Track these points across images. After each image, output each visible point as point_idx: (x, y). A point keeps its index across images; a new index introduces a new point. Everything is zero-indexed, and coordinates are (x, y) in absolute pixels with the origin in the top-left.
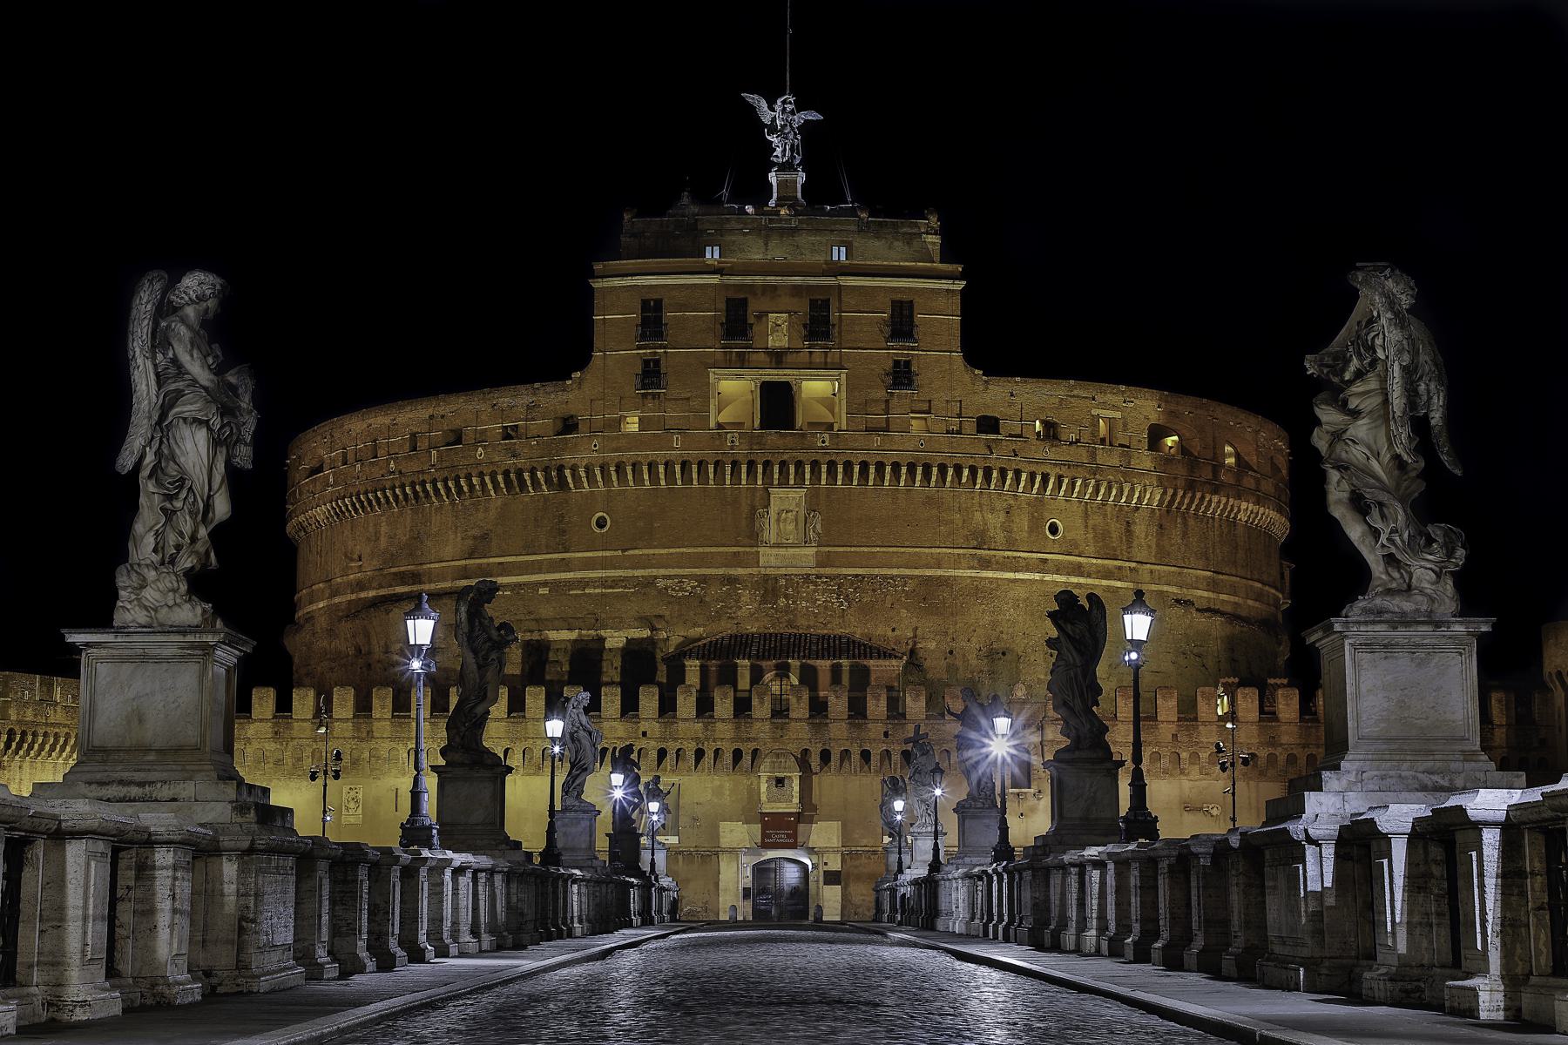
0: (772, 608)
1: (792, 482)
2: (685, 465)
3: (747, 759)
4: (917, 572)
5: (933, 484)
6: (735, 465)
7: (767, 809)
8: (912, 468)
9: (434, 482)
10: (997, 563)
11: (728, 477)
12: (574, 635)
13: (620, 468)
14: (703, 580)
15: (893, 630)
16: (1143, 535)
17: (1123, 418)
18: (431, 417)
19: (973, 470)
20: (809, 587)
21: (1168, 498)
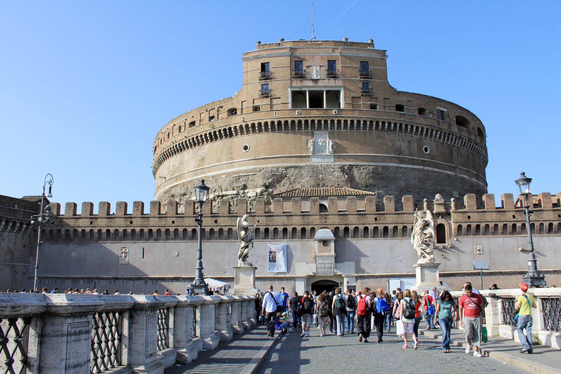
0: (316, 178)
1: (323, 128)
2: (279, 123)
3: (308, 233)
4: (375, 164)
5: (380, 129)
6: (300, 122)
7: (318, 254)
8: (371, 122)
9: (186, 141)
10: (406, 161)
11: (297, 128)
12: (235, 192)
13: (253, 125)
14: (287, 168)
15: (367, 187)
16: (456, 156)
17: (447, 112)
18: (186, 120)
19: (395, 124)
20: (331, 170)
21: (463, 143)
